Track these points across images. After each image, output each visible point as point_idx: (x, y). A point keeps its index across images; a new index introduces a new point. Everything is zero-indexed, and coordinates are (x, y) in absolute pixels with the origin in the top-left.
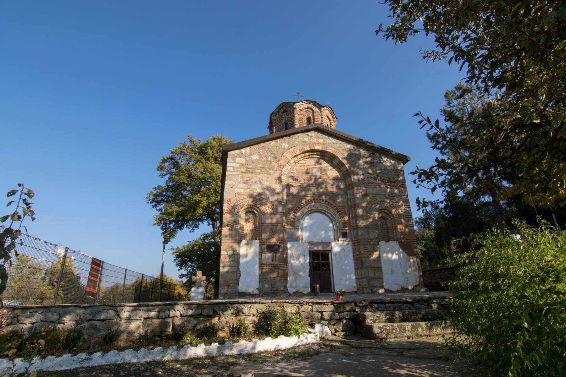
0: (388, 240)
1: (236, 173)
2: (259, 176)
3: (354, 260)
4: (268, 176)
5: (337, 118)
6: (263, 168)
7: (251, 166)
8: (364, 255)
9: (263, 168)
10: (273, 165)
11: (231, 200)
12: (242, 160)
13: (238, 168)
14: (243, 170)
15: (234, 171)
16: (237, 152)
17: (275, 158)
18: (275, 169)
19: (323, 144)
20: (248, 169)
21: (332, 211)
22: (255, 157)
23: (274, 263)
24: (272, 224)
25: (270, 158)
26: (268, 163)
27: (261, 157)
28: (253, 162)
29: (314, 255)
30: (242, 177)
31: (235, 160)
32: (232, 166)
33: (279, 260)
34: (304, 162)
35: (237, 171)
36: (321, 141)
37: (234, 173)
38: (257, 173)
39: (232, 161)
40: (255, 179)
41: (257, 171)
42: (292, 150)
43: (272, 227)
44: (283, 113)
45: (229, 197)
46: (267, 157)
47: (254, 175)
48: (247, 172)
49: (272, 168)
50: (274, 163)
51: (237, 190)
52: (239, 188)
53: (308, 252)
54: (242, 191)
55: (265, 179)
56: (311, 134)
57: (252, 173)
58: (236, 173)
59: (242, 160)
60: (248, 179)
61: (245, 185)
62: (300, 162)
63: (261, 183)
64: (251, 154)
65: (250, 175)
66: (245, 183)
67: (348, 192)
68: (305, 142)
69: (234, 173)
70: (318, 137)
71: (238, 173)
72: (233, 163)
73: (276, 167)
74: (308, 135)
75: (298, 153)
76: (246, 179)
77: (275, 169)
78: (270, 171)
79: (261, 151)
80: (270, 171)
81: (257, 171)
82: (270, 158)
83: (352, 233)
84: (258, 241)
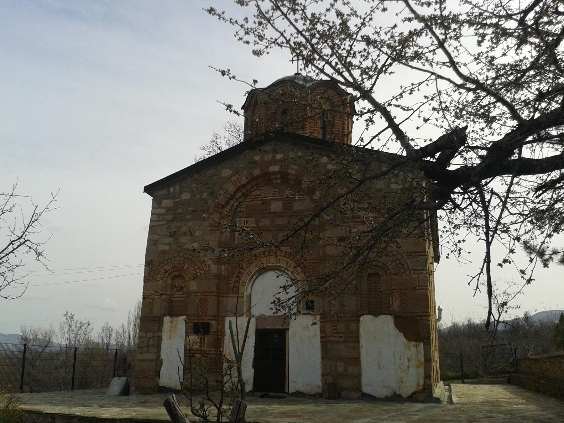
0: (376, 313)
1: (161, 223)
2: (189, 224)
3: (322, 345)
7: (180, 211)
8: (330, 339)
10: (208, 204)
13: (163, 215)
14: (170, 217)
17: (212, 194)
19: (281, 161)
22: (186, 196)
29: (261, 334)
34: (259, 193)
35: (162, 220)
37: (159, 223)
38: (188, 220)
40: (184, 229)
42: (234, 178)
48: (174, 220)
50: (210, 202)
52: (163, 244)
53: (254, 331)
54: (167, 248)
57: (181, 221)
58: (161, 223)
60: (176, 230)
61: (171, 239)
62: (253, 194)
63: (191, 234)
64: (181, 192)
65: (179, 224)
68: (256, 162)
69: (159, 223)
72: (158, 208)
73: (212, 208)
74: (260, 150)
76: (173, 230)
78: (204, 215)
79: (194, 185)
80: (204, 215)
82: (205, 195)
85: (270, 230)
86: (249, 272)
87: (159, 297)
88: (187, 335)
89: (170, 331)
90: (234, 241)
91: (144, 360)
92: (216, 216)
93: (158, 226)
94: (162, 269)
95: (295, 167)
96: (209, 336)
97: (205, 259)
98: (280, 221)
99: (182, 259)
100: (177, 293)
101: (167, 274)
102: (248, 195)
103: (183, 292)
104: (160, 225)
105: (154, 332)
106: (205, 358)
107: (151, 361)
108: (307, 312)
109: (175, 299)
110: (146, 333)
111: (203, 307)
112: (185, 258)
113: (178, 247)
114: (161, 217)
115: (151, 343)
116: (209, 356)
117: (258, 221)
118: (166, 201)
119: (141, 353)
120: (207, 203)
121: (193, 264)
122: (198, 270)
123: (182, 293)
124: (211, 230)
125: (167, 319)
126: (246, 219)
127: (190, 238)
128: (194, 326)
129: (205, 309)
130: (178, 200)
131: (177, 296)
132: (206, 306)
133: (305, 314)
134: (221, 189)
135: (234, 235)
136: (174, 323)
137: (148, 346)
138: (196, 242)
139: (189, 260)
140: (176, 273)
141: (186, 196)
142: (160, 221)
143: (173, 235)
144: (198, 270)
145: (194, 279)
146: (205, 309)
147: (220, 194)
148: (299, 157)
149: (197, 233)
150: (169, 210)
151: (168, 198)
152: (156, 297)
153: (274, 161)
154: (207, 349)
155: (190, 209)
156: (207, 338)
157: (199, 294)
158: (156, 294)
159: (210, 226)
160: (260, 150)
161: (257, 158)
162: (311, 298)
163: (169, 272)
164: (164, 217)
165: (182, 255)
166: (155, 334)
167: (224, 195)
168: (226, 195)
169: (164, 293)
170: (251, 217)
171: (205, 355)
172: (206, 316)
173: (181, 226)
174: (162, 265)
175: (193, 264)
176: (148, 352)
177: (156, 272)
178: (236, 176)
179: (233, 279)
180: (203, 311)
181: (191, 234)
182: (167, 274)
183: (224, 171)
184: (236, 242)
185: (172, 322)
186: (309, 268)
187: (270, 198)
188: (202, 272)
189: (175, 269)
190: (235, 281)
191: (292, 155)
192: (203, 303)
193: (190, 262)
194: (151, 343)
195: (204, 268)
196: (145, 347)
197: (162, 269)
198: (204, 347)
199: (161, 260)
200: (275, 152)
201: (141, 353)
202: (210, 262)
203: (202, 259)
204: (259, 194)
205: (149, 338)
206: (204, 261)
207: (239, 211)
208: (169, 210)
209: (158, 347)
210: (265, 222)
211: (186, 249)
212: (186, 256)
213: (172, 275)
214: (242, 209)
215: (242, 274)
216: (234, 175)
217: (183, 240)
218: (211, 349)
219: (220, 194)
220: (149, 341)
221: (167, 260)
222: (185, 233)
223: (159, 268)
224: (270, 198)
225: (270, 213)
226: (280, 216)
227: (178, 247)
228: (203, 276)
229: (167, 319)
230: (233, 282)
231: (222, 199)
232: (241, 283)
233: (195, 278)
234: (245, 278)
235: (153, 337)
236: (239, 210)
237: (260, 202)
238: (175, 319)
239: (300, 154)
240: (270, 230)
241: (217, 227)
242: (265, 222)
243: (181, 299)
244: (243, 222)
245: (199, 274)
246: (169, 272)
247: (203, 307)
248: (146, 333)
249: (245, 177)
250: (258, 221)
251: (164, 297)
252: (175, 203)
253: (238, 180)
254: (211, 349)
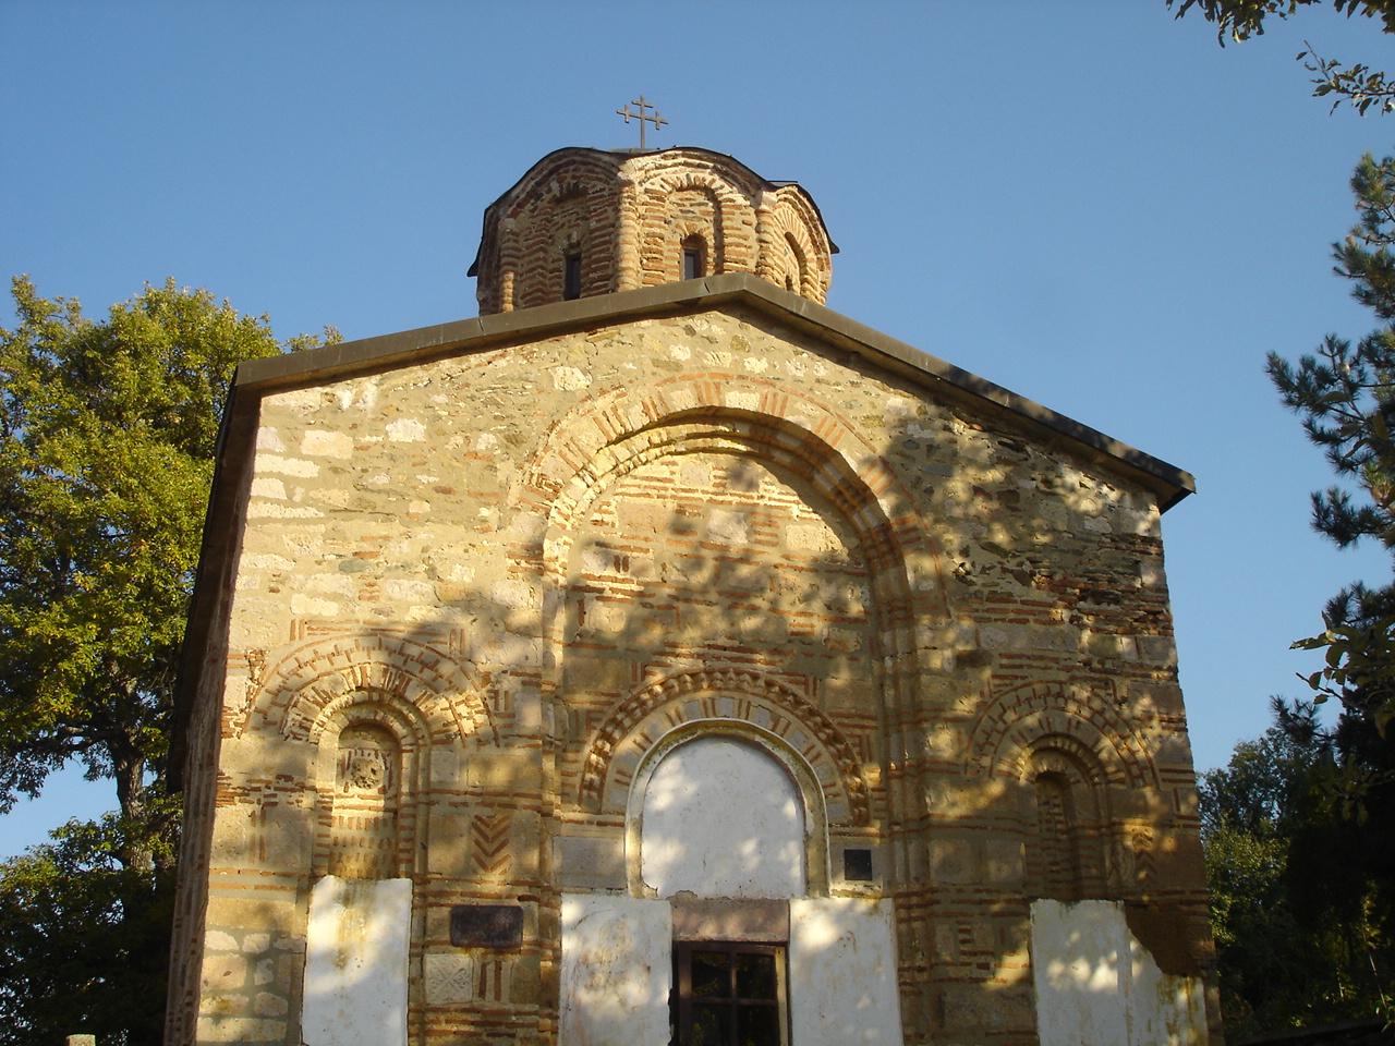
0: (1072, 894)
1: (299, 512)
2: (423, 535)
3: (902, 993)
4: (474, 537)
5: (835, 250)
6: (447, 491)
7: (381, 480)
8: (952, 972)
9: (447, 491)
10: (501, 477)
11: (270, 659)
12: (331, 444)
13: (310, 483)
14: (340, 497)
15: (290, 502)
16: (312, 397)
17: (513, 440)
18: (512, 500)
19: (766, 382)
20: (365, 495)
21: (799, 737)
22: (406, 431)
23: (489, 1003)
24: (485, 796)
25: (486, 441)
26: (475, 464)
27: (436, 430)
28: (394, 455)
29: (692, 960)
30: (332, 536)
31: (293, 446)
32: (280, 476)
33: (514, 988)
34: (664, 472)
35: (305, 503)
36: (756, 365)
38: (411, 519)
39: (280, 447)
40: (402, 550)
41: (416, 507)
42: (603, 403)
43: (485, 812)
44: (558, 201)
45: (260, 643)
46: (469, 432)
47: (396, 528)
48: (362, 507)
49: (496, 497)
50: (505, 469)
51: (301, 606)
52: (314, 594)
53: (668, 947)
54: (330, 610)
55: (461, 551)
56: (702, 323)
58: (299, 512)
59: (331, 444)
60: (366, 547)
61: (347, 579)
62: (641, 471)
63: (432, 573)
64: (385, 415)
65: (377, 528)
66: (345, 568)
67: (886, 638)
68: (677, 366)
70: (740, 345)
71: (311, 512)
72: (287, 455)
73: (515, 492)
74: (690, 331)
75: (638, 421)
76: (354, 547)
77: (512, 500)
78: (484, 512)
79: (441, 399)
81: (416, 507)
82: (486, 441)
83: (899, 855)
84: (404, 883)
93: (287, 522)
148: (818, 381)
150: (335, 470)
153: (741, 377)
154: (511, 1007)
161: (681, 353)
168: (570, 456)
171: (503, 1029)
173: (387, 538)
178: (609, 398)
186: (849, 741)
198: (498, 997)
214: (607, 518)
216: (603, 392)
218: (527, 1008)
219: (547, 448)
236: (597, 516)
249: (639, 408)
253: (615, 409)
254: (527, 1008)
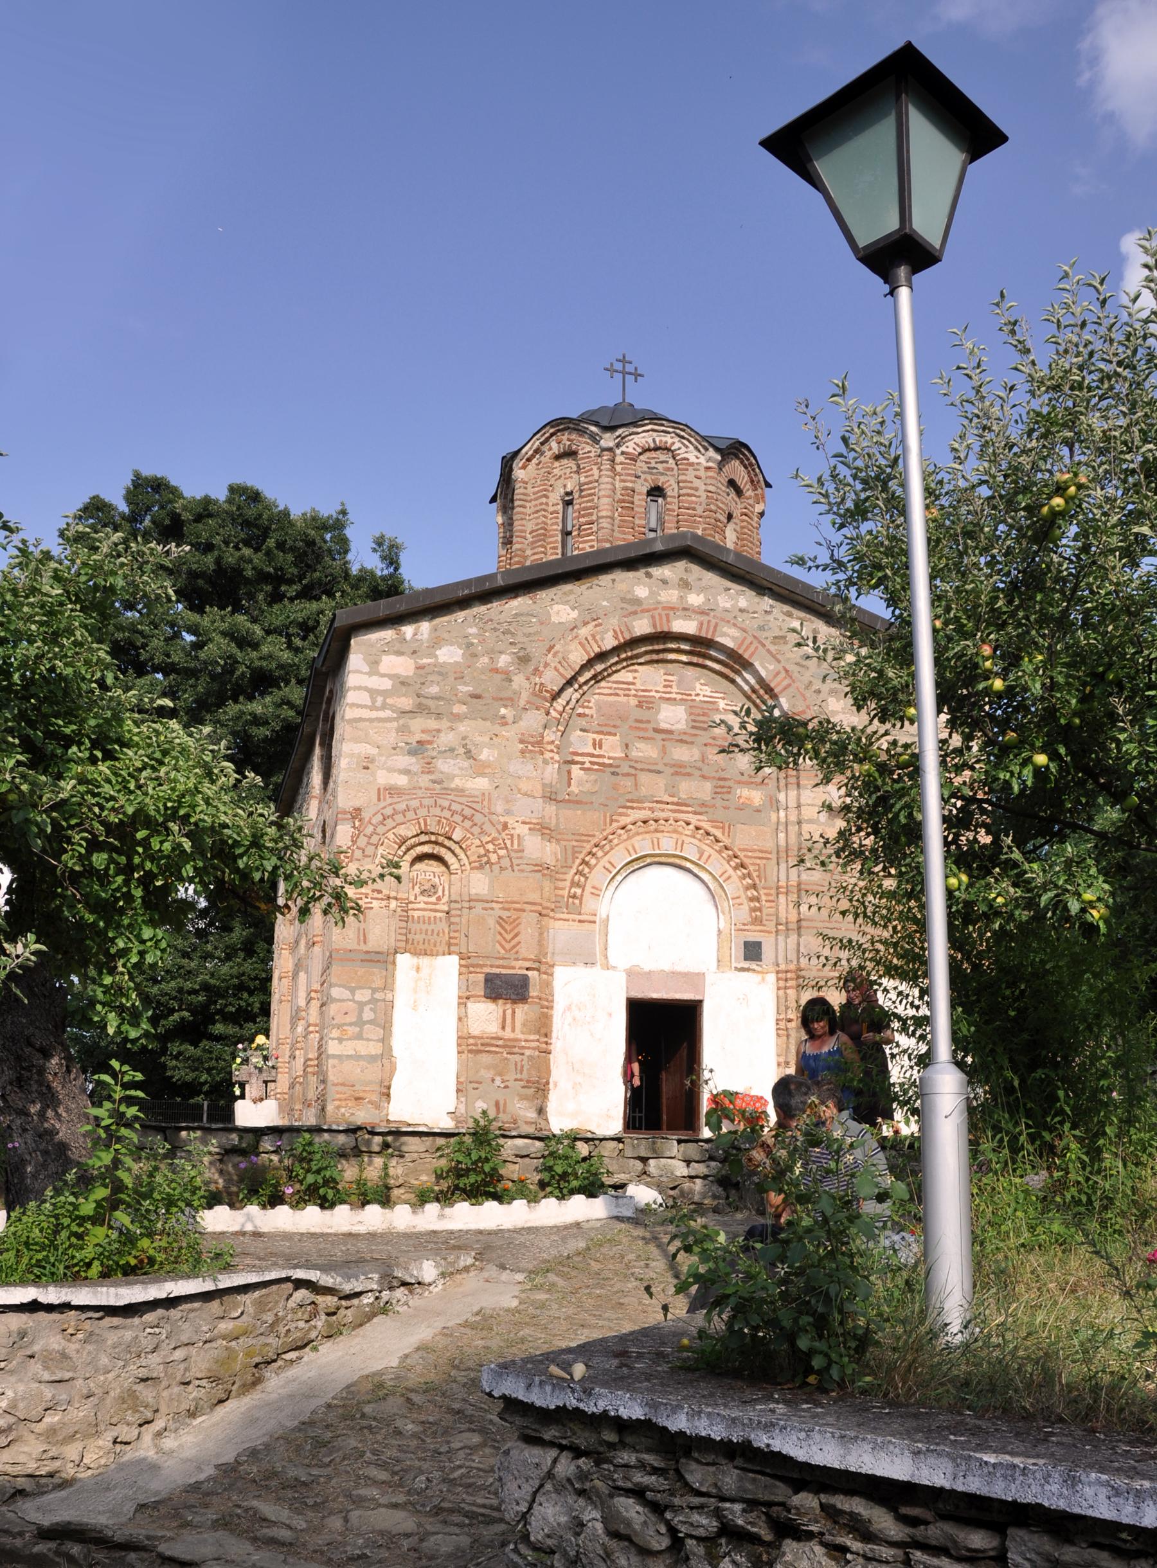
2: (463, 728)
4: (497, 728)
5: (768, 485)
6: (478, 697)
7: (434, 690)
9: (478, 697)
10: (515, 686)
11: (366, 815)
12: (402, 665)
13: (384, 693)
14: (406, 703)
15: (373, 708)
16: (387, 634)
17: (524, 660)
18: (522, 703)
20: (422, 699)
21: (718, 864)
22: (449, 654)
23: (508, 1034)
25: (504, 660)
26: (499, 677)
27: (471, 653)
28: (441, 671)
30: (403, 730)
31: (374, 670)
32: (366, 689)
33: (524, 1025)
35: (384, 707)
36: (695, 599)
37: (374, 714)
38: (458, 718)
39: (366, 669)
40: (447, 739)
41: (459, 709)
42: (584, 632)
43: (505, 914)
44: (558, 457)
45: (358, 804)
46: (493, 653)
47: (444, 724)
48: (420, 709)
49: (509, 701)
50: (519, 681)
51: (383, 778)
52: (390, 770)
54: (402, 781)
55: (487, 739)
56: (658, 571)
57: (439, 716)
59: (402, 665)
60: (425, 737)
61: (413, 760)
62: (615, 677)
63: (469, 754)
64: (437, 642)
65: (432, 724)
66: (412, 753)
67: (782, 796)
68: (638, 601)
69: (374, 714)
70: (685, 585)
71: (387, 713)
72: (370, 674)
73: (525, 696)
74: (649, 575)
75: (609, 643)
76: (418, 737)
77: (522, 703)
78: (503, 711)
79: (473, 630)
80: (503, 711)
81: (459, 709)
83: (781, 944)
84: (454, 959)
85: (659, 772)
86: (608, 866)
87: (384, 903)
88: (464, 1001)
89: (415, 991)
90: (569, 785)
91: (349, 1057)
92: (533, 720)
93: (371, 720)
94: (390, 835)
95: (733, 632)
96: (526, 1007)
97: (511, 821)
98: (681, 754)
99: (447, 814)
100: (421, 898)
101: (403, 848)
102: (604, 678)
103: (439, 899)
104: (379, 720)
105: (374, 991)
106: (517, 1058)
107: (372, 1059)
108: (746, 965)
109: (416, 914)
110: (352, 991)
111: (508, 937)
112: (454, 813)
113: (434, 782)
114: (380, 700)
115: (368, 1015)
116: (528, 1052)
117: (627, 746)
118: (392, 658)
119: (340, 1040)
120: (511, 681)
121: (476, 830)
122: (490, 847)
123: (433, 899)
124: (522, 752)
125: (404, 961)
126: (597, 737)
127: (466, 764)
128: (486, 980)
129: (513, 942)
130: (425, 661)
131: (422, 906)
132: (516, 935)
133: (743, 970)
134: (549, 650)
135: (569, 772)
136: (425, 971)
137: (360, 1023)
138: (483, 775)
139: (465, 818)
140: (426, 849)
141: (449, 654)
142: (377, 709)
143: (418, 749)
144: (490, 847)
145: (481, 867)
146: (513, 942)
147: (546, 665)
148: (741, 610)
149: (485, 755)
150: (403, 683)
151: (399, 653)
152: (375, 904)
153: (685, 609)
154: (521, 1036)
155: (465, 689)
156: (521, 1011)
157: (494, 905)
158: (376, 895)
159: (522, 742)
160: (649, 575)
161: (641, 592)
162: (752, 937)
163: (409, 843)
164: (389, 701)
165: (446, 804)
166: (378, 996)
167: (556, 669)
168: (561, 670)
169: (393, 894)
170: (610, 734)
171: (516, 1050)
172: (517, 959)
173: (439, 731)
174: (390, 823)
175: (476, 830)
176: (359, 1037)
177: (375, 839)
178: (591, 626)
179: (569, 877)
180: (508, 946)
181: (469, 754)
182: (403, 848)
183: (556, 607)
184: (574, 788)
185: (418, 969)
186: (751, 868)
187: (658, 695)
188: (502, 852)
189: (423, 838)
190: (572, 882)
191: (724, 602)
192: (508, 928)
193: (468, 824)
194: (368, 1015)
195: (508, 842)
196: (351, 1024)
197: (390, 835)
198: (513, 1030)
199: (388, 811)
200: (685, 585)
201: (340, 1040)
202: (523, 830)
203: (502, 819)
204: (631, 680)
205: (361, 1005)
206: (505, 826)
207: (580, 715)
208: (403, 683)
209: (386, 1026)
210: (645, 751)
211: (457, 789)
212: (455, 807)
213: (413, 853)
214: (587, 711)
215: (591, 868)
216: (585, 624)
217: (445, 766)
218: (532, 1037)
219: (546, 665)
220: (361, 1011)
221: (404, 813)
222: (452, 750)
223: (381, 829)
224: (658, 695)
225: (657, 730)
226: (681, 741)
227: (434, 782)
228: (506, 862)
229: (404, 961)
230: (568, 883)
231: (552, 679)
232: (588, 889)
233: (483, 863)
234: (598, 876)
235: (373, 1001)
236: (580, 710)
237: (633, 701)
238: (424, 961)
239: (743, 603)
240: (659, 772)
241: (533, 746)
242: (645, 751)
243: (432, 914)
244: (590, 743)
245: (494, 858)
246: (409, 843)
247: (508, 937)
248: (352, 991)
249: (611, 633)
250: (627, 746)
251: (393, 904)
252: (420, 668)
253: (594, 636)
254: (532, 1037)
